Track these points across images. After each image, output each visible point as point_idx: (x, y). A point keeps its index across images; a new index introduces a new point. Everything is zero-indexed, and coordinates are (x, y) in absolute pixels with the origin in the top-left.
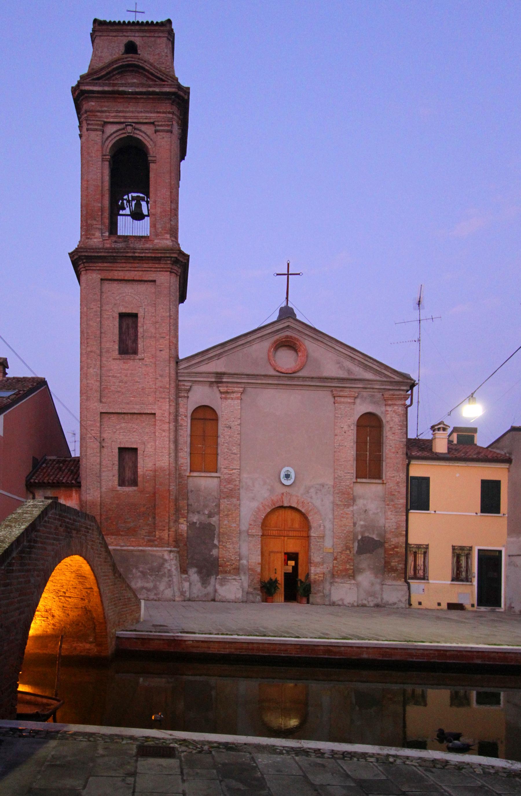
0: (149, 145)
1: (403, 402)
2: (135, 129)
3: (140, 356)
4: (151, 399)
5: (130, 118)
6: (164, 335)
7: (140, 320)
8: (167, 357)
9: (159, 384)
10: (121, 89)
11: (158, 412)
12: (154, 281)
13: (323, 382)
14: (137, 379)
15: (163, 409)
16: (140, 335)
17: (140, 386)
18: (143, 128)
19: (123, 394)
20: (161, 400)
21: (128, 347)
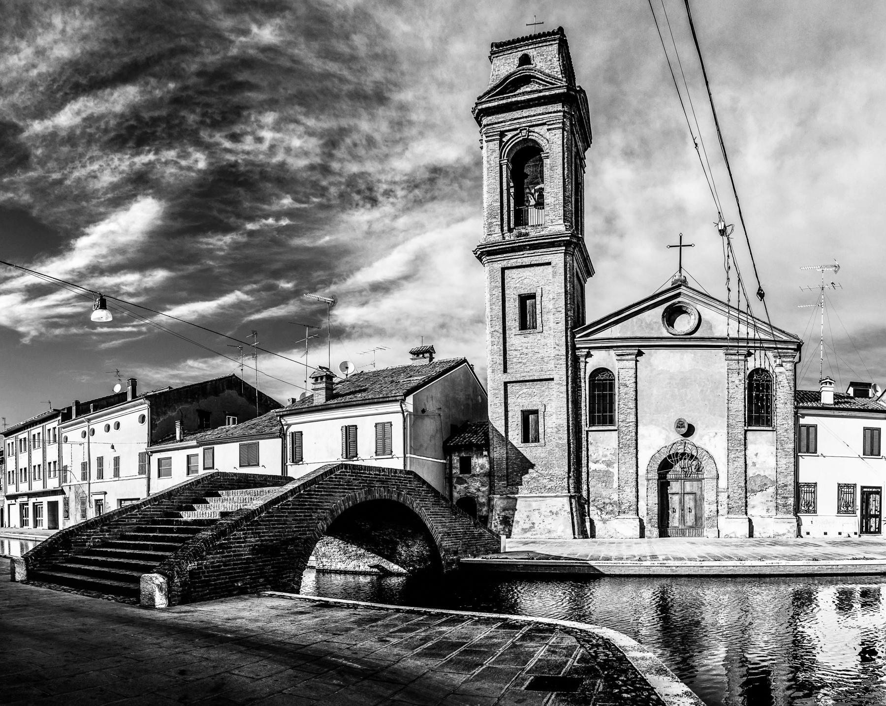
0: (543, 143)
1: (791, 359)
2: (530, 132)
3: (539, 329)
4: (551, 365)
5: (524, 123)
6: (560, 309)
7: (538, 298)
8: (564, 328)
9: (557, 352)
10: (514, 100)
11: (556, 377)
12: (549, 264)
13: (711, 343)
14: (536, 350)
15: (560, 373)
16: (538, 311)
17: (539, 356)
18: (536, 129)
19: (524, 364)
20: (558, 366)
21: (526, 323)
